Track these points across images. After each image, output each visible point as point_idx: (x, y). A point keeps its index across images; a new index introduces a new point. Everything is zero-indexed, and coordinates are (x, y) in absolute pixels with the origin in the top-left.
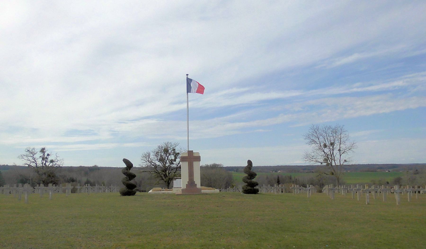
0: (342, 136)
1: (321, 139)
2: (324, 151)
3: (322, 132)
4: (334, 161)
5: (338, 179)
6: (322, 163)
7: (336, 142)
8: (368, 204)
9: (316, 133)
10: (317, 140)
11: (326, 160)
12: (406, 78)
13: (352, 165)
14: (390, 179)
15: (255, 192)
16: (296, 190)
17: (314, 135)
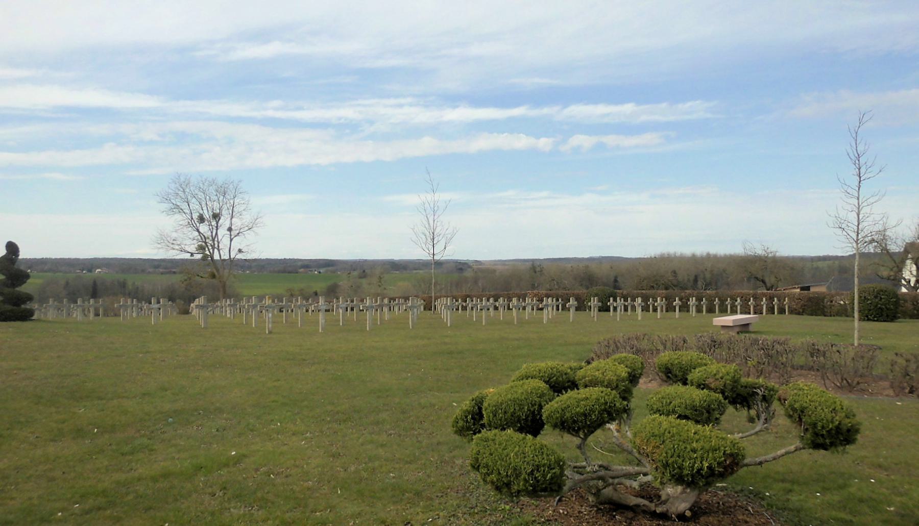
0: (237, 201)
1: (195, 205)
2: (198, 230)
3: (196, 192)
4: (219, 250)
5: (224, 286)
6: (192, 255)
7: (223, 212)
8: (270, 332)
9: (184, 192)
10: (184, 206)
11: (201, 248)
12: (359, 105)
13: (255, 260)
14: (320, 286)
15: (26, 316)
16: (130, 313)
17: (179, 195)
